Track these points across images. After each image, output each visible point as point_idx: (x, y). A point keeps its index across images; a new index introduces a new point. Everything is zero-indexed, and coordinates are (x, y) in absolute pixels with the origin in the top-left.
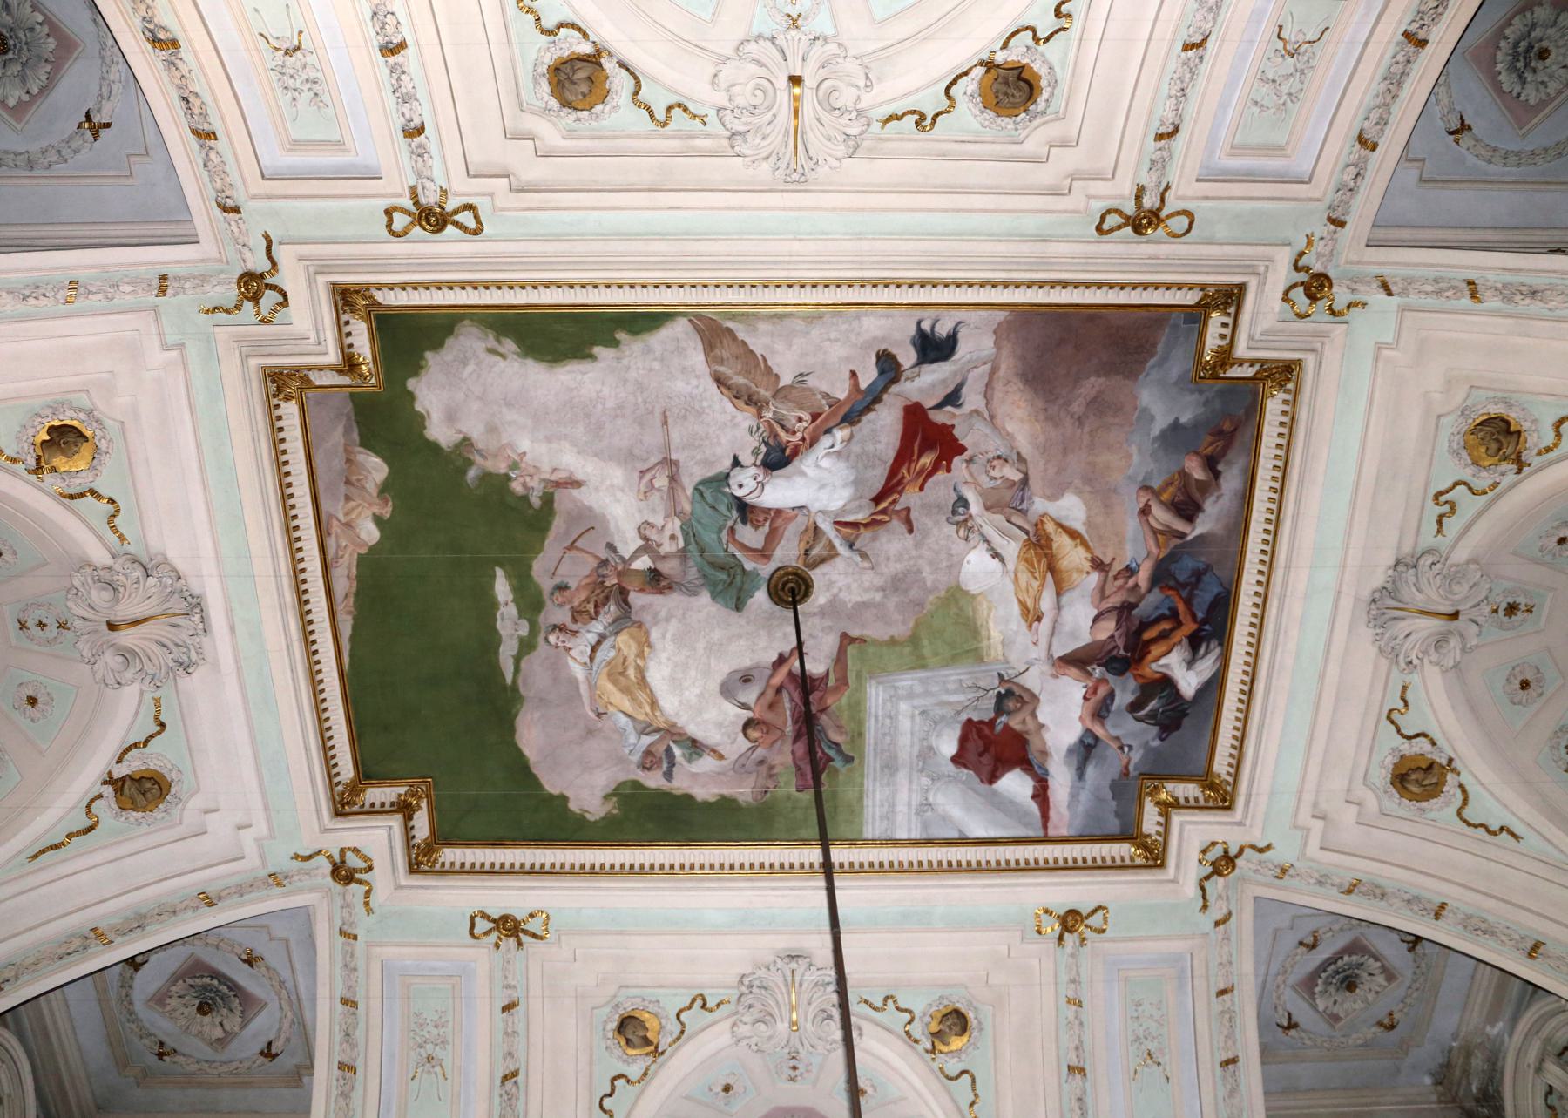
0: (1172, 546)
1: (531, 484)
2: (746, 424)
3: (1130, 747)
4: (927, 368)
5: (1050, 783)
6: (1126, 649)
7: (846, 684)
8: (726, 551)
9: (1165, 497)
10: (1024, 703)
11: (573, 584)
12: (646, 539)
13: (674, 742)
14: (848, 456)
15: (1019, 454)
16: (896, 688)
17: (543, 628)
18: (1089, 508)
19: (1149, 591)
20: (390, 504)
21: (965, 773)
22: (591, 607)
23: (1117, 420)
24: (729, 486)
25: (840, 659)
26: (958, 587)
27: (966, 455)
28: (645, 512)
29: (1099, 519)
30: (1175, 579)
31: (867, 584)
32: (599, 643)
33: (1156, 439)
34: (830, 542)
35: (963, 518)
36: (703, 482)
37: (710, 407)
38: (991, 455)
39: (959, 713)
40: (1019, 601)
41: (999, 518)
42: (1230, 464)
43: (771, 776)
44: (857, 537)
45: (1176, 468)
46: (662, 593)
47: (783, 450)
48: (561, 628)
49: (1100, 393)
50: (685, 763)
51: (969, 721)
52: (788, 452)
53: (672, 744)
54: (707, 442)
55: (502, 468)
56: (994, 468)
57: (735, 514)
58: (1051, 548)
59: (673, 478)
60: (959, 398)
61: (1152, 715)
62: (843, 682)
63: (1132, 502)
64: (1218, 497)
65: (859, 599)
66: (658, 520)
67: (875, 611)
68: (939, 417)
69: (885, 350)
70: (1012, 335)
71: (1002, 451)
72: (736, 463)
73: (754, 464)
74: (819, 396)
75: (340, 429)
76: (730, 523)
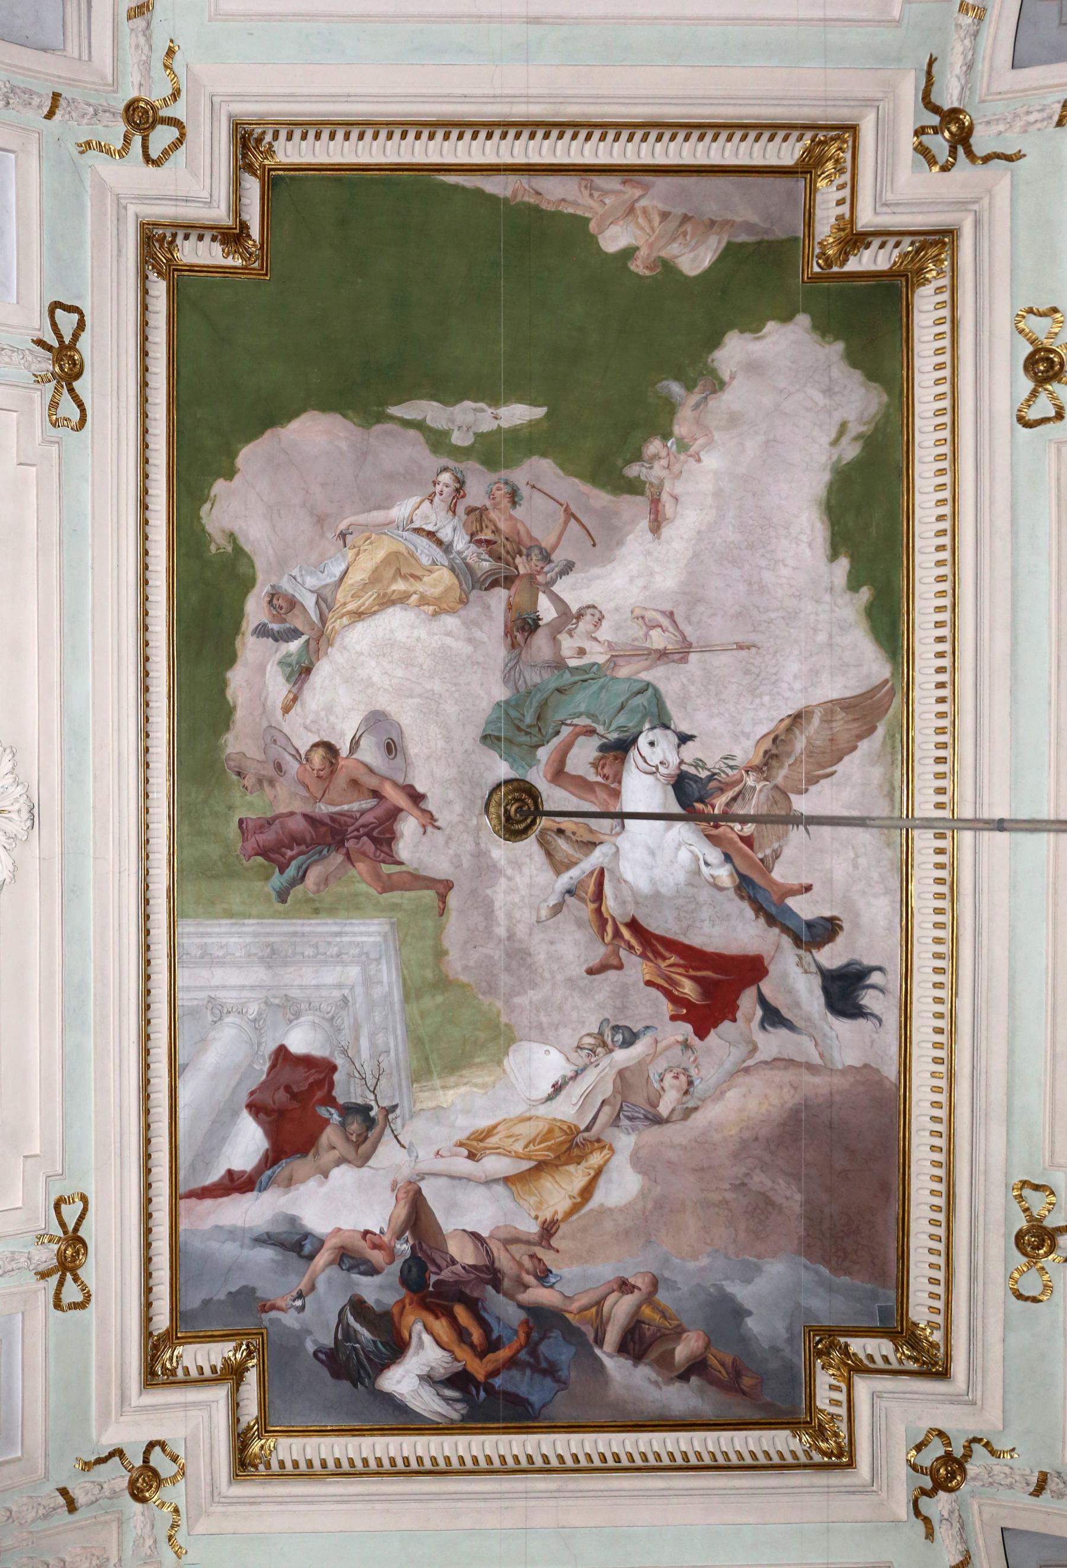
0: (584, 1328)
1: (657, 465)
2: (738, 752)
3: (302, 1308)
4: (817, 982)
5: (249, 1195)
6: (439, 1283)
7: (384, 890)
8: (563, 723)
9: (647, 1311)
10: (357, 1145)
11: (519, 512)
12: (580, 615)
13: (307, 642)
14: (693, 886)
15: (696, 1109)
16: (378, 960)
17: (462, 466)
18: (621, 1210)
19: (521, 1306)
20: (647, 273)
21: (263, 1067)
22: (487, 535)
23: (742, 1235)
24: (652, 728)
25: (418, 881)
26: (511, 1040)
27: (695, 1040)
28: (617, 617)
29: (609, 1225)
30: (541, 1339)
31: (517, 915)
32: (439, 543)
33: (720, 1289)
34: (576, 864)
35: (609, 1041)
36: (657, 696)
37: (763, 705)
38: (693, 1072)
39: (345, 1052)
40: (495, 1127)
41: (607, 1090)
42: (701, 1392)
43: (260, 781)
44: (583, 900)
45: (685, 1319)
46: (506, 635)
47: (701, 800)
48: (460, 486)
49: (780, 1209)
50: (278, 656)
51: (334, 1068)
52: (699, 806)
53: (304, 638)
54: (713, 701)
55: (680, 429)
56: (676, 1077)
57: (614, 736)
58: (566, 1164)
59: (663, 655)
60: (773, 1025)
61: (349, 1335)
62: (387, 885)
65: (497, 905)
66: (605, 633)
67: (481, 927)
68: (747, 1001)
69: (841, 928)
70: (861, 1088)
71: (699, 1086)
72: (684, 739)
73: (682, 762)
74: (776, 846)
75: (754, 219)
76: (600, 729)
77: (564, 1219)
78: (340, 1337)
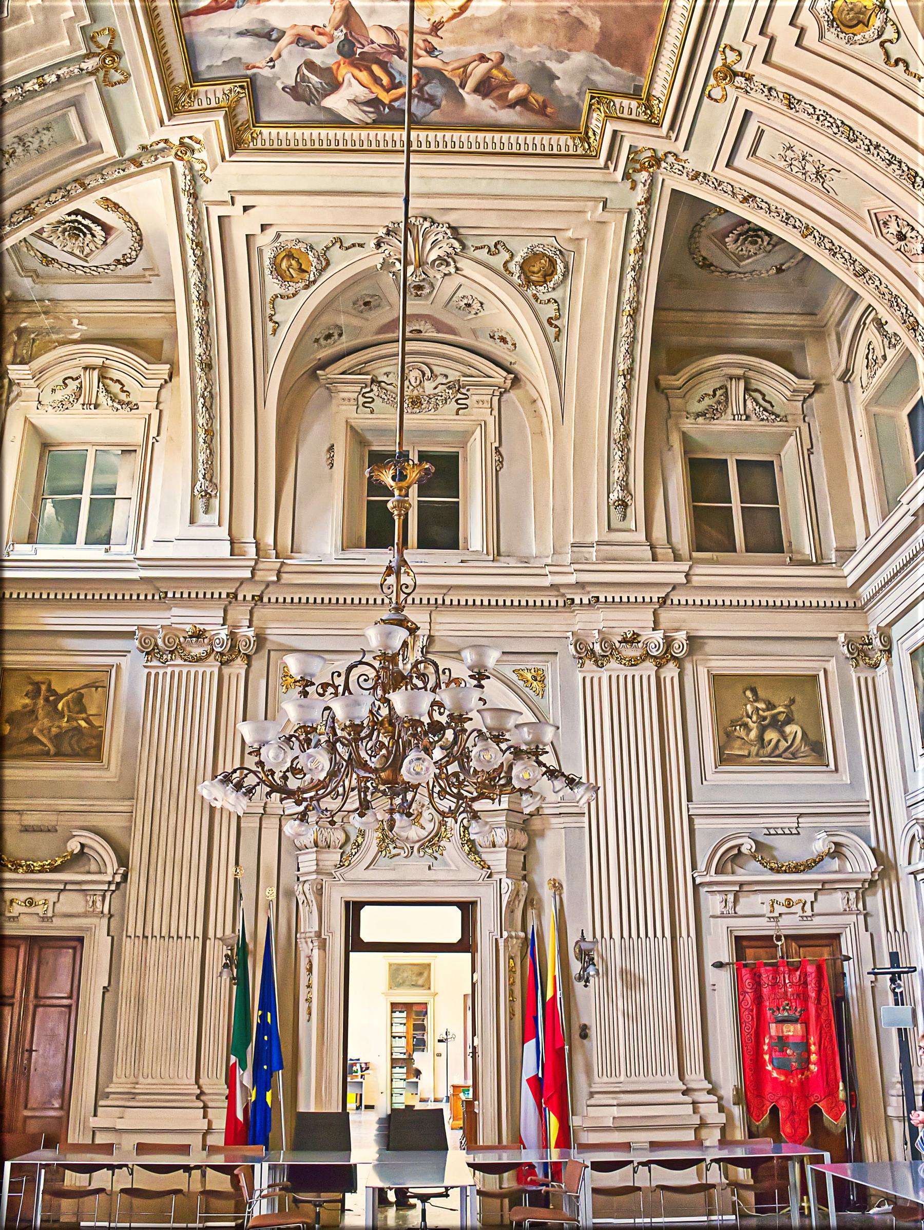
0: (454, 79)
9: (495, 72)
29: (477, 26)
30: (425, 84)
33: (543, 64)
42: (521, 114)
45: (517, 77)
61: (304, 79)
63: (492, 47)
64: (494, 108)
77: (447, 21)
78: (298, 80)
